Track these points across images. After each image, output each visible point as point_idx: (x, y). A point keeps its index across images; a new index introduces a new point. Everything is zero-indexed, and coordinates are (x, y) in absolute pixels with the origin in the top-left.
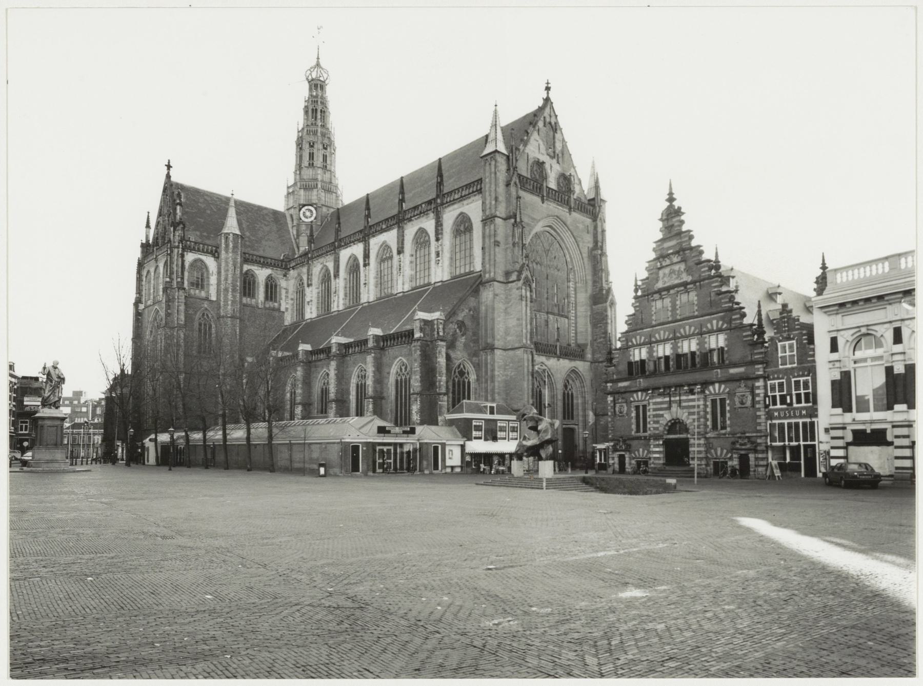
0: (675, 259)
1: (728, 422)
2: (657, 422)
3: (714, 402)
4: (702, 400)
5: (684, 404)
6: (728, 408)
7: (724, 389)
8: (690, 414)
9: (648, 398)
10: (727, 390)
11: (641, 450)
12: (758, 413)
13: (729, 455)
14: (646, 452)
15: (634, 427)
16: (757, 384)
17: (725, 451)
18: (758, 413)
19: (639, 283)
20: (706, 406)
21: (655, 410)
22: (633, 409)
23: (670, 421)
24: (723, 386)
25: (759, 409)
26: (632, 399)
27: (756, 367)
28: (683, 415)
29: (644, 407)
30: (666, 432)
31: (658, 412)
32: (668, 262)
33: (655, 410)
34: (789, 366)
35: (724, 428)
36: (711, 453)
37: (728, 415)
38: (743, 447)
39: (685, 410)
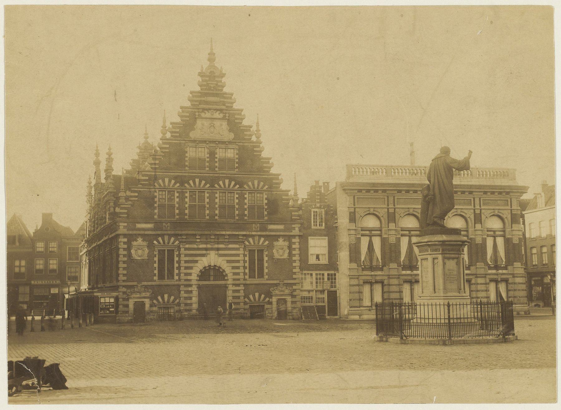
0: (217, 115)
1: (266, 271)
2: (191, 268)
3: (252, 252)
4: (242, 249)
6: (266, 259)
7: (264, 241)
8: (228, 262)
9: (177, 242)
10: (267, 242)
11: (166, 296)
12: (294, 264)
13: (267, 299)
14: (172, 298)
15: (156, 272)
16: (294, 240)
17: (263, 296)
18: (294, 264)
19: (169, 125)
20: (245, 255)
21: (186, 255)
22: (156, 253)
24: (262, 239)
25: (295, 261)
26: (155, 242)
27: (293, 226)
28: (221, 262)
29: (171, 252)
30: (198, 278)
31: (191, 258)
32: (208, 115)
33: (186, 255)
34: (318, 227)
35: (261, 275)
36: (249, 299)
37: (266, 265)
38: (282, 293)
39: (223, 258)
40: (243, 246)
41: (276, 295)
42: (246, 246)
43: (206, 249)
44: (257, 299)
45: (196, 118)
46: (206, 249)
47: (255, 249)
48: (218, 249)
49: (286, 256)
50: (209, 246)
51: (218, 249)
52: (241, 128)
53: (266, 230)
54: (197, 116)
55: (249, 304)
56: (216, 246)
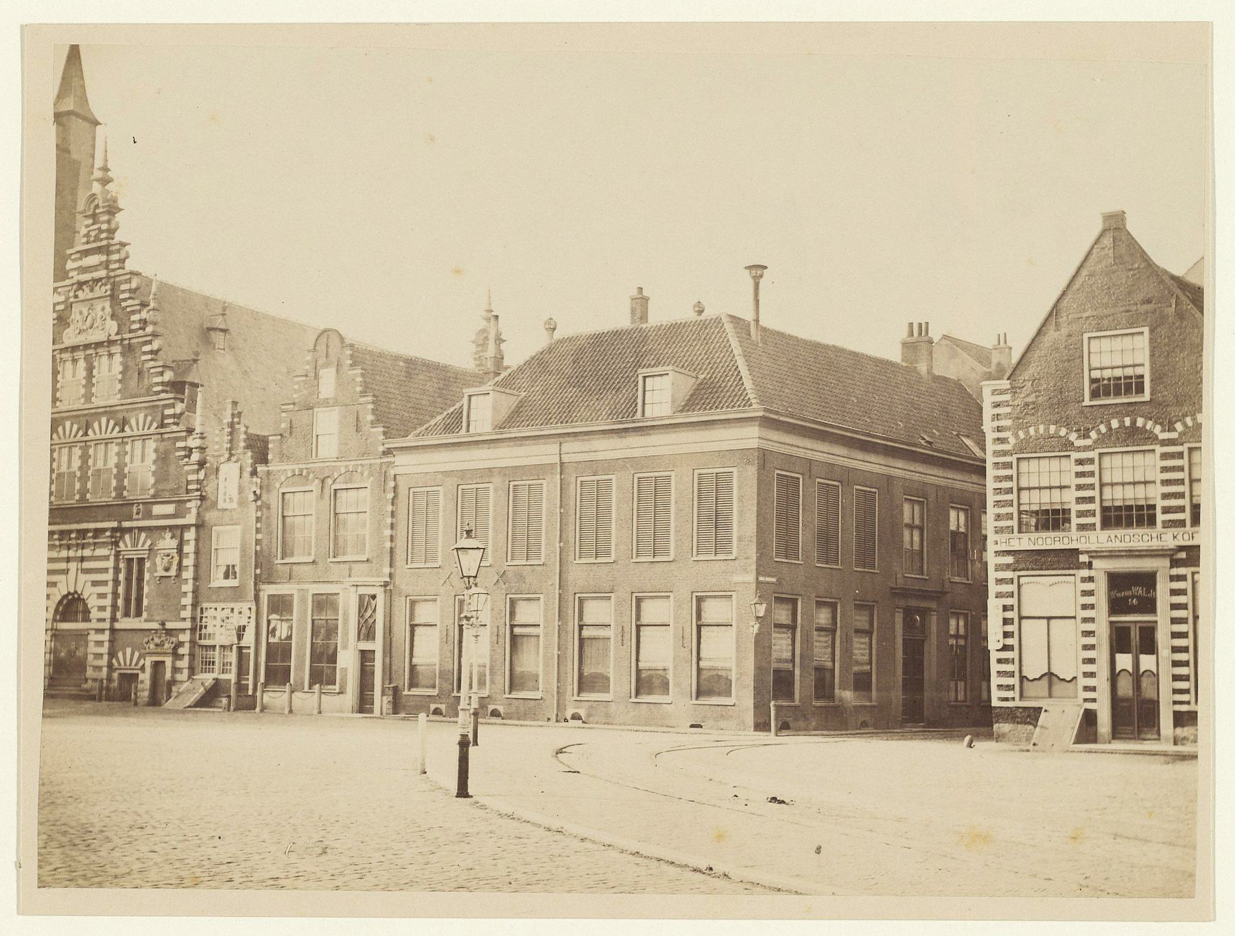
5: (86, 565)
8: (95, 583)
20: (117, 570)
23: (65, 597)
40: (113, 552)
41: (151, 654)
42: (120, 551)
43: (68, 560)
44: (128, 663)
45: (72, 304)
46: (68, 560)
47: (131, 557)
48: (82, 559)
49: (173, 572)
50: (72, 553)
51: (82, 559)
52: (128, 309)
53: (149, 515)
54: (72, 300)
55: (118, 671)
56: (79, 553)
